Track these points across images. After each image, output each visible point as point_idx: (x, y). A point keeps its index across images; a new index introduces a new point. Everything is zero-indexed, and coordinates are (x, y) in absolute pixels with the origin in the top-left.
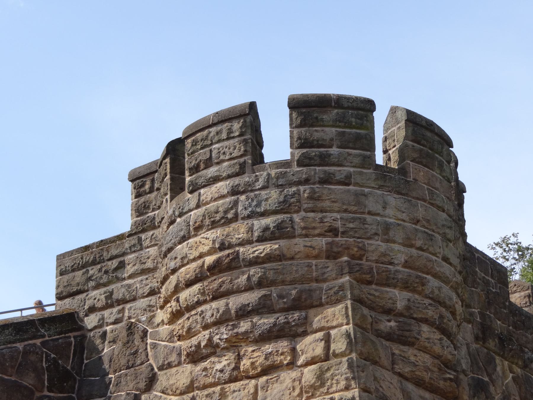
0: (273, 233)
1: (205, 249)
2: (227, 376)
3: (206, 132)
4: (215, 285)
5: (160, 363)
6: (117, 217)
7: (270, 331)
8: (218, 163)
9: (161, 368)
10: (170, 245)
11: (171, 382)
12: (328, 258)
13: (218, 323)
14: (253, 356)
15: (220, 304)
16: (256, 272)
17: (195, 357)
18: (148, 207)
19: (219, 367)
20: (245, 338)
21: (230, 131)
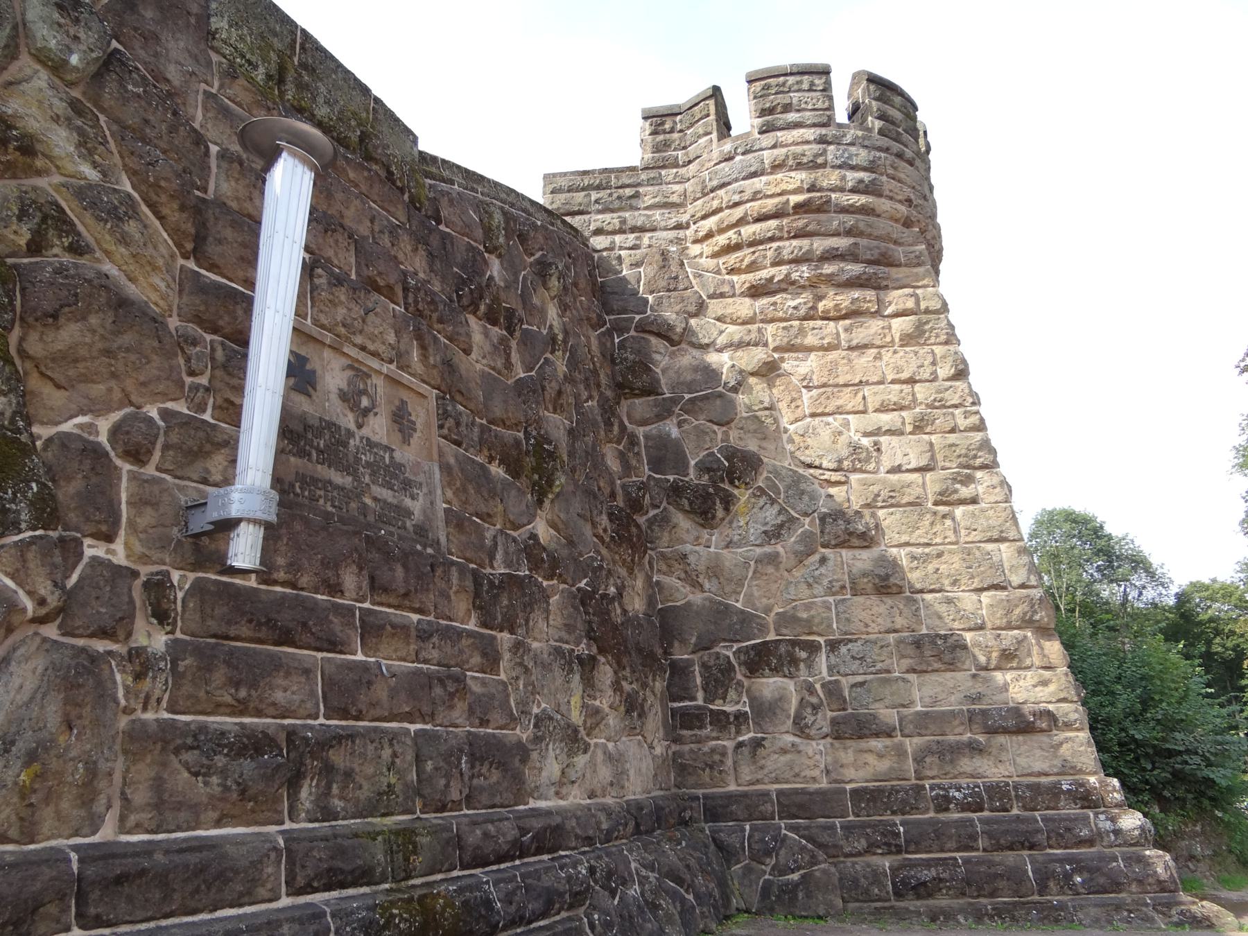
0: (867, 186)
1: (791, 187)
2: (802, 312)
3: (782, 79)
4: (800, 223)
5: (711, 291)
6: (626, 148)
7: (858, 277)
8: (798, 111)
9: (710, 297)
10: (726, 180)
11: (730, 311)
12: (904, 225)
13: (796, 261)
14: (833, 300)
15: (805, 243)
16: (850, 220)
17: (755, 292)
18: (669, 146)
19: (793, 303)
20: (830, 280)
21: (812, 84)
